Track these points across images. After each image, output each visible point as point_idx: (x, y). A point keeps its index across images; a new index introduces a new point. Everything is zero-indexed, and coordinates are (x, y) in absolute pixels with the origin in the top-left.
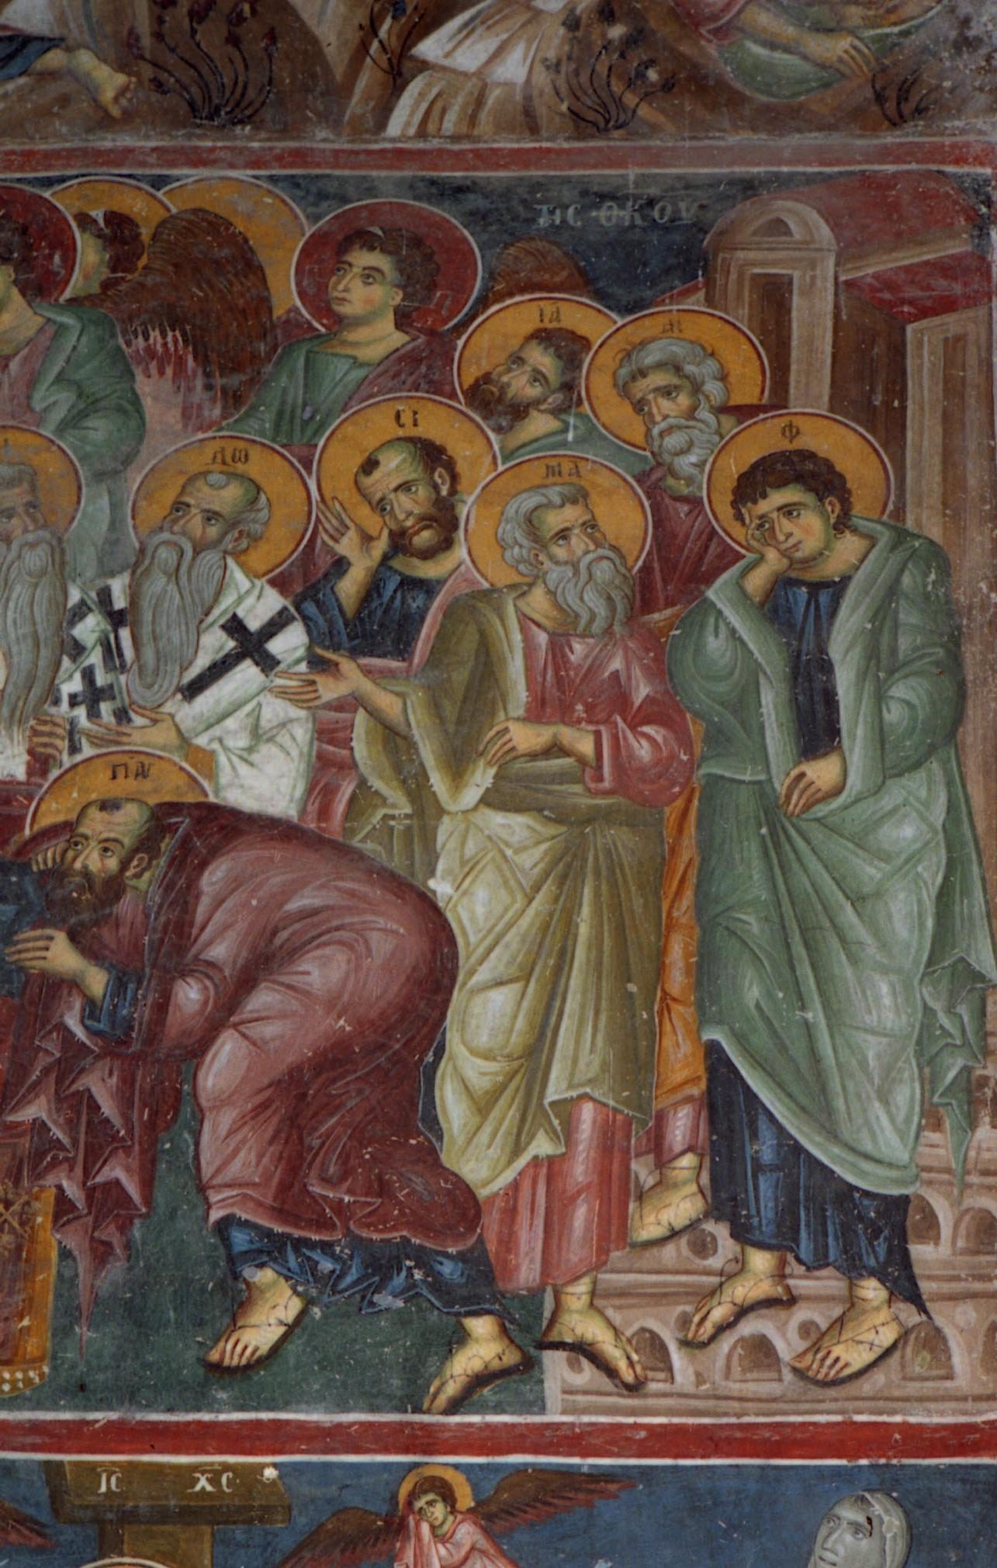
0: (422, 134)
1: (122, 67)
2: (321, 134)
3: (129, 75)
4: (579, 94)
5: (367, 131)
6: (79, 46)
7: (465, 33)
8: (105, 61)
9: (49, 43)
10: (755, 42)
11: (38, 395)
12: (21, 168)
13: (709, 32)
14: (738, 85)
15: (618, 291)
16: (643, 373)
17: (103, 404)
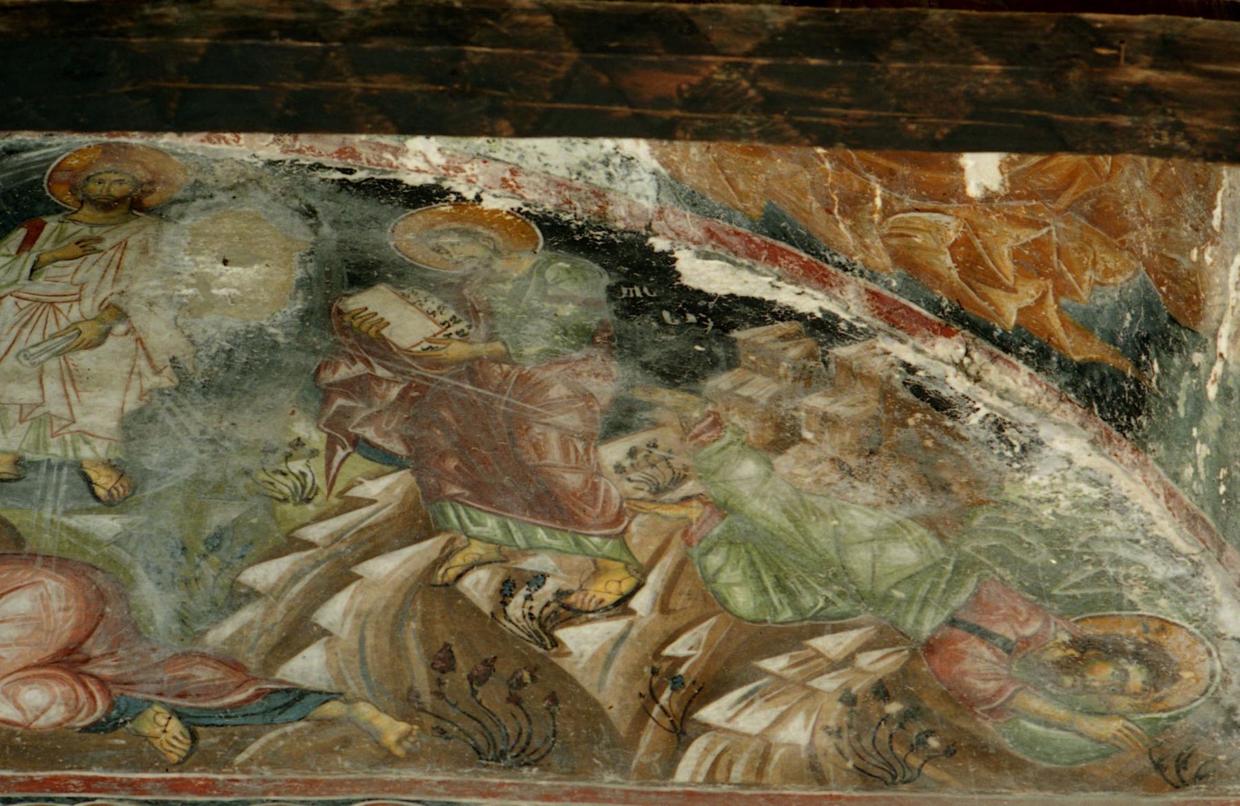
0: (711, 778)
1: (403, 718)
2: (612, 777)
3: (410, 723)
4: (863, 754)
5: (657, 777)
6: (358, 700)
7: (744, 703)
8: (386, 712)
9: (326, 696)
10: (1030, 720)
13: (983, 711)
14: (1018, 753)
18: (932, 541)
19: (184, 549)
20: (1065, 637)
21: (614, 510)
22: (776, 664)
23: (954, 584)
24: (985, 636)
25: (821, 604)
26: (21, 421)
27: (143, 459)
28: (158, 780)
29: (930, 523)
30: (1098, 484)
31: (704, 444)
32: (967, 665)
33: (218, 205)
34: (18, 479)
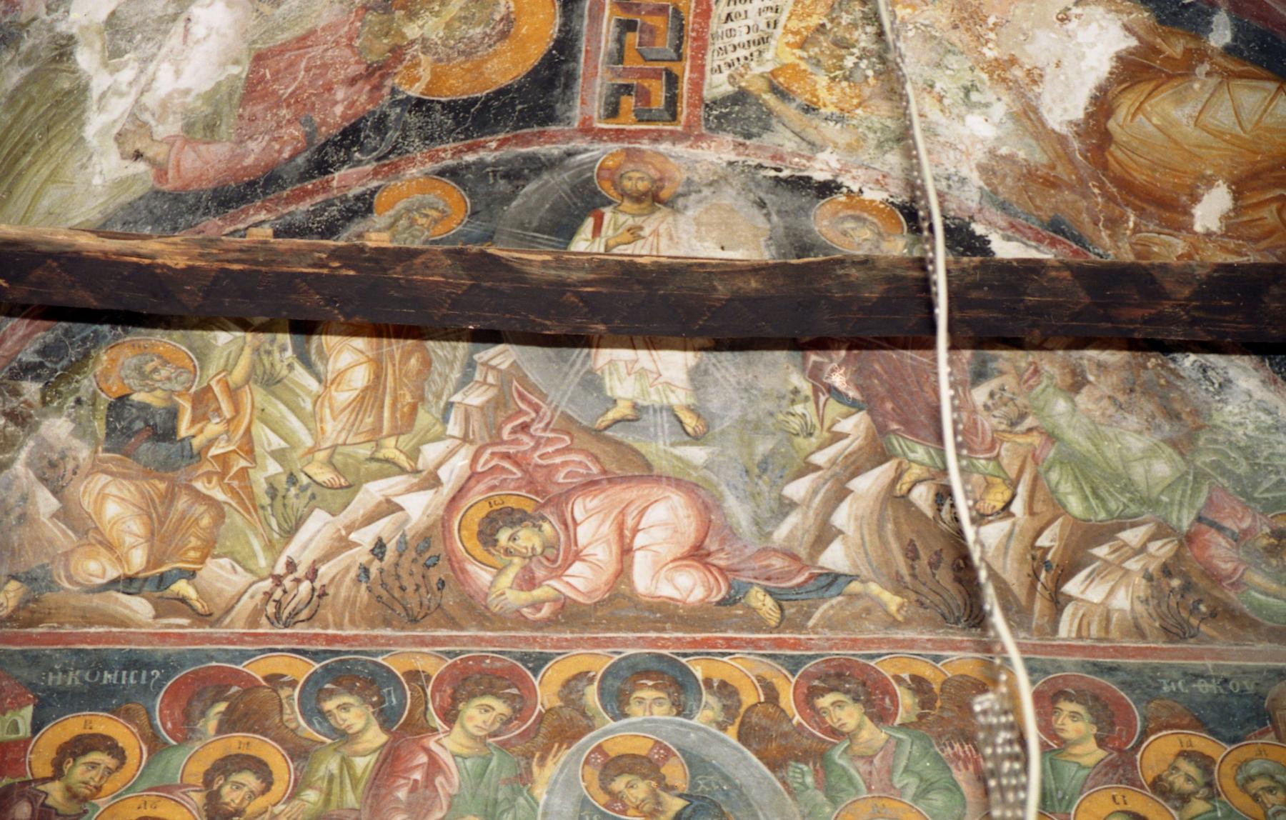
0: (1079, 637)
1: (897, 593)
9: (851, 578)
11: (896, 778)
12: (852, 648)
14: (1253, 615)
15: (1223, 731)
16: (1251, 779)
17: (936, 785)
18: (1177, 458)
19: (747, 472)
20: (1268, 530)
21: (989, 439)
22: (1102, 551)
23: (1196, 491)
24: (1220, 529)
25: (1121, 508)
26: (629, 374)
27: (709, 405)
28: (766, 639)
29: (1173, 444)
30: (1270, 413)
31: (1031, 388)
32: (1213, 551)
33: (706, 198)
34: (637, 420)
